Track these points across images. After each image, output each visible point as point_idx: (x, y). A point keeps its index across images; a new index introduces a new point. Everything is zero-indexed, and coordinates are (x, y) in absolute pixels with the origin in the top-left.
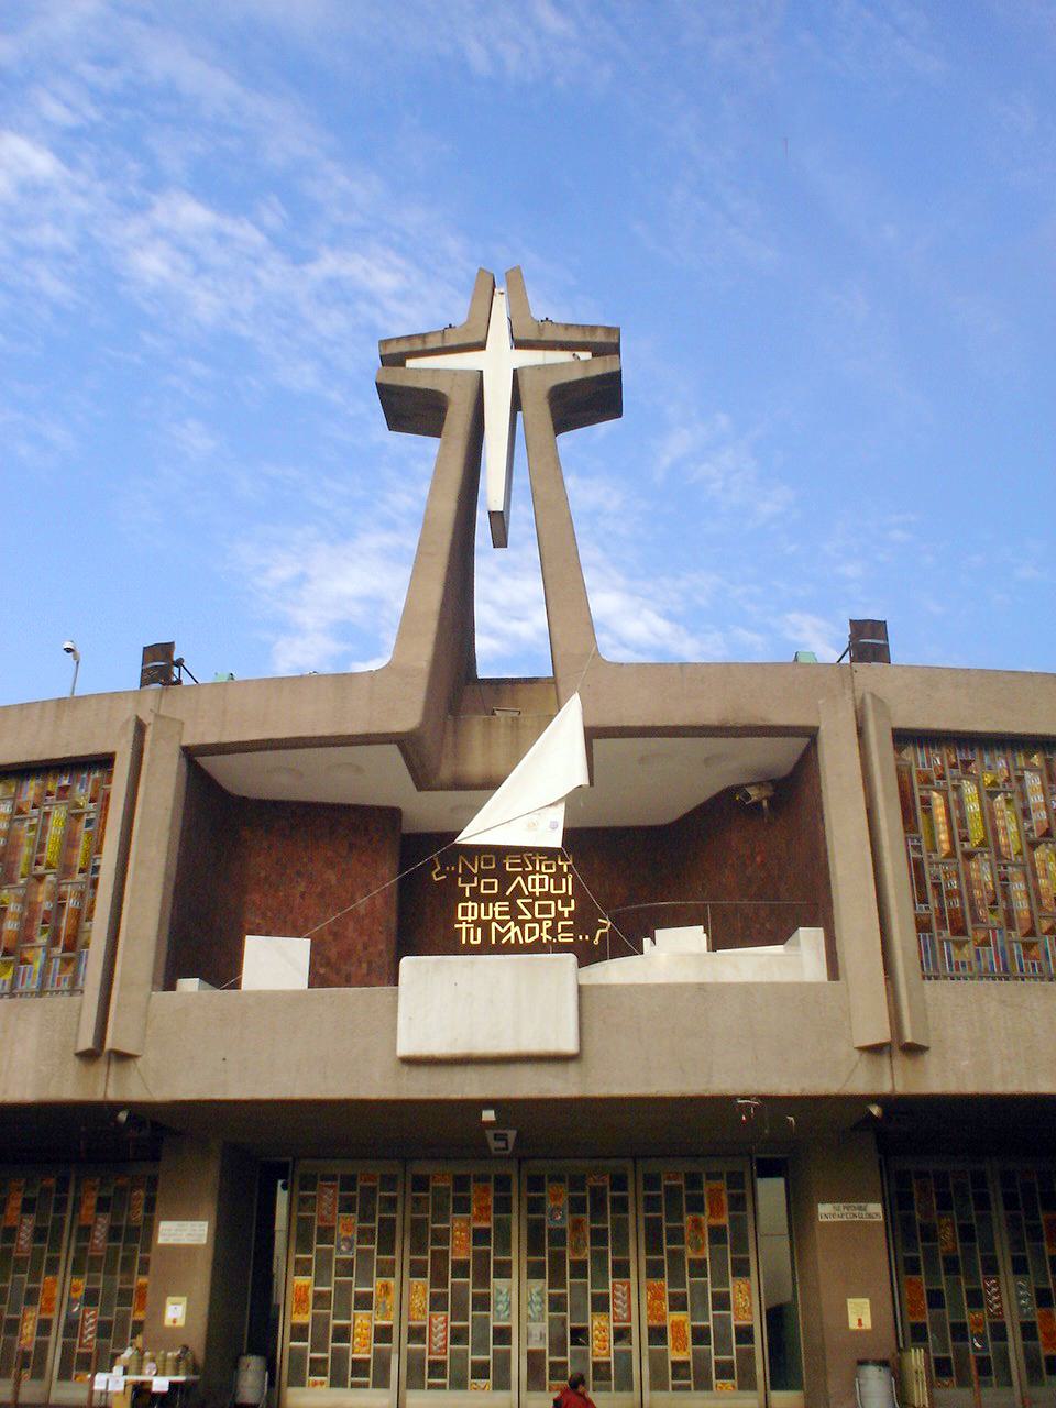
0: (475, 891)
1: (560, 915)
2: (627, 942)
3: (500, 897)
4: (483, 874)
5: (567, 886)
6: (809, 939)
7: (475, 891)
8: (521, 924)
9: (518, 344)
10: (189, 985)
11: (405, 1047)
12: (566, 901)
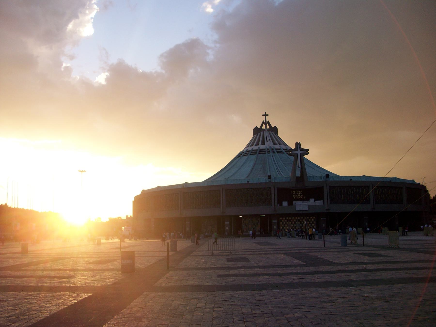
0: (295, 194)
1: (301, 196)
2: (308, 199)
3: (297, 194)
4: (295, 193)
5: (302, 194)
6: (322, 201)
7: (295, 194)
8: (298, 197)
9: (300, 150)
10: (279, 205)
11: (296, 210)
12: (302, 195)
